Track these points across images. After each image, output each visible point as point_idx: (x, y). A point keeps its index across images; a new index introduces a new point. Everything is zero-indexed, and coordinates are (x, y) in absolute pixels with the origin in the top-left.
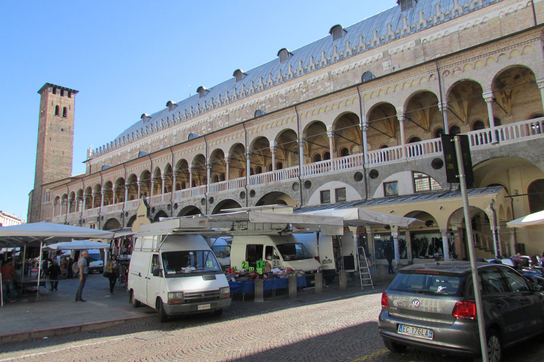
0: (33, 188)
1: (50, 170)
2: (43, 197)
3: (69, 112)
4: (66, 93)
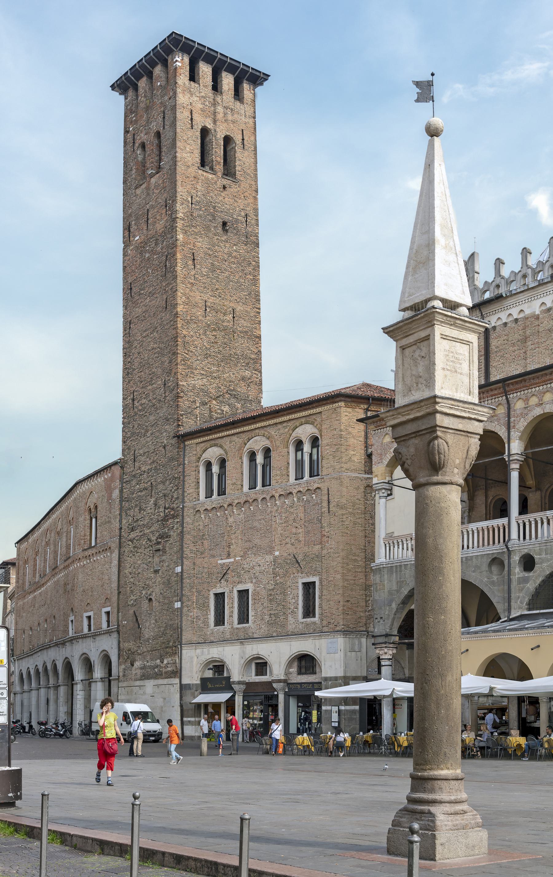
0: (113, 451)
1: (198, 382)
2: (190, 481)
3: (241, 158)
4: (227, 81)
